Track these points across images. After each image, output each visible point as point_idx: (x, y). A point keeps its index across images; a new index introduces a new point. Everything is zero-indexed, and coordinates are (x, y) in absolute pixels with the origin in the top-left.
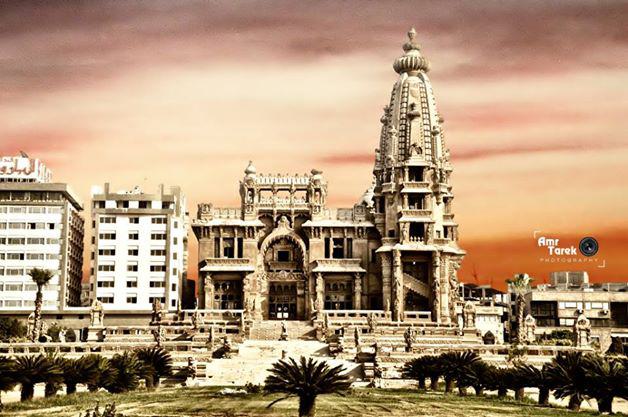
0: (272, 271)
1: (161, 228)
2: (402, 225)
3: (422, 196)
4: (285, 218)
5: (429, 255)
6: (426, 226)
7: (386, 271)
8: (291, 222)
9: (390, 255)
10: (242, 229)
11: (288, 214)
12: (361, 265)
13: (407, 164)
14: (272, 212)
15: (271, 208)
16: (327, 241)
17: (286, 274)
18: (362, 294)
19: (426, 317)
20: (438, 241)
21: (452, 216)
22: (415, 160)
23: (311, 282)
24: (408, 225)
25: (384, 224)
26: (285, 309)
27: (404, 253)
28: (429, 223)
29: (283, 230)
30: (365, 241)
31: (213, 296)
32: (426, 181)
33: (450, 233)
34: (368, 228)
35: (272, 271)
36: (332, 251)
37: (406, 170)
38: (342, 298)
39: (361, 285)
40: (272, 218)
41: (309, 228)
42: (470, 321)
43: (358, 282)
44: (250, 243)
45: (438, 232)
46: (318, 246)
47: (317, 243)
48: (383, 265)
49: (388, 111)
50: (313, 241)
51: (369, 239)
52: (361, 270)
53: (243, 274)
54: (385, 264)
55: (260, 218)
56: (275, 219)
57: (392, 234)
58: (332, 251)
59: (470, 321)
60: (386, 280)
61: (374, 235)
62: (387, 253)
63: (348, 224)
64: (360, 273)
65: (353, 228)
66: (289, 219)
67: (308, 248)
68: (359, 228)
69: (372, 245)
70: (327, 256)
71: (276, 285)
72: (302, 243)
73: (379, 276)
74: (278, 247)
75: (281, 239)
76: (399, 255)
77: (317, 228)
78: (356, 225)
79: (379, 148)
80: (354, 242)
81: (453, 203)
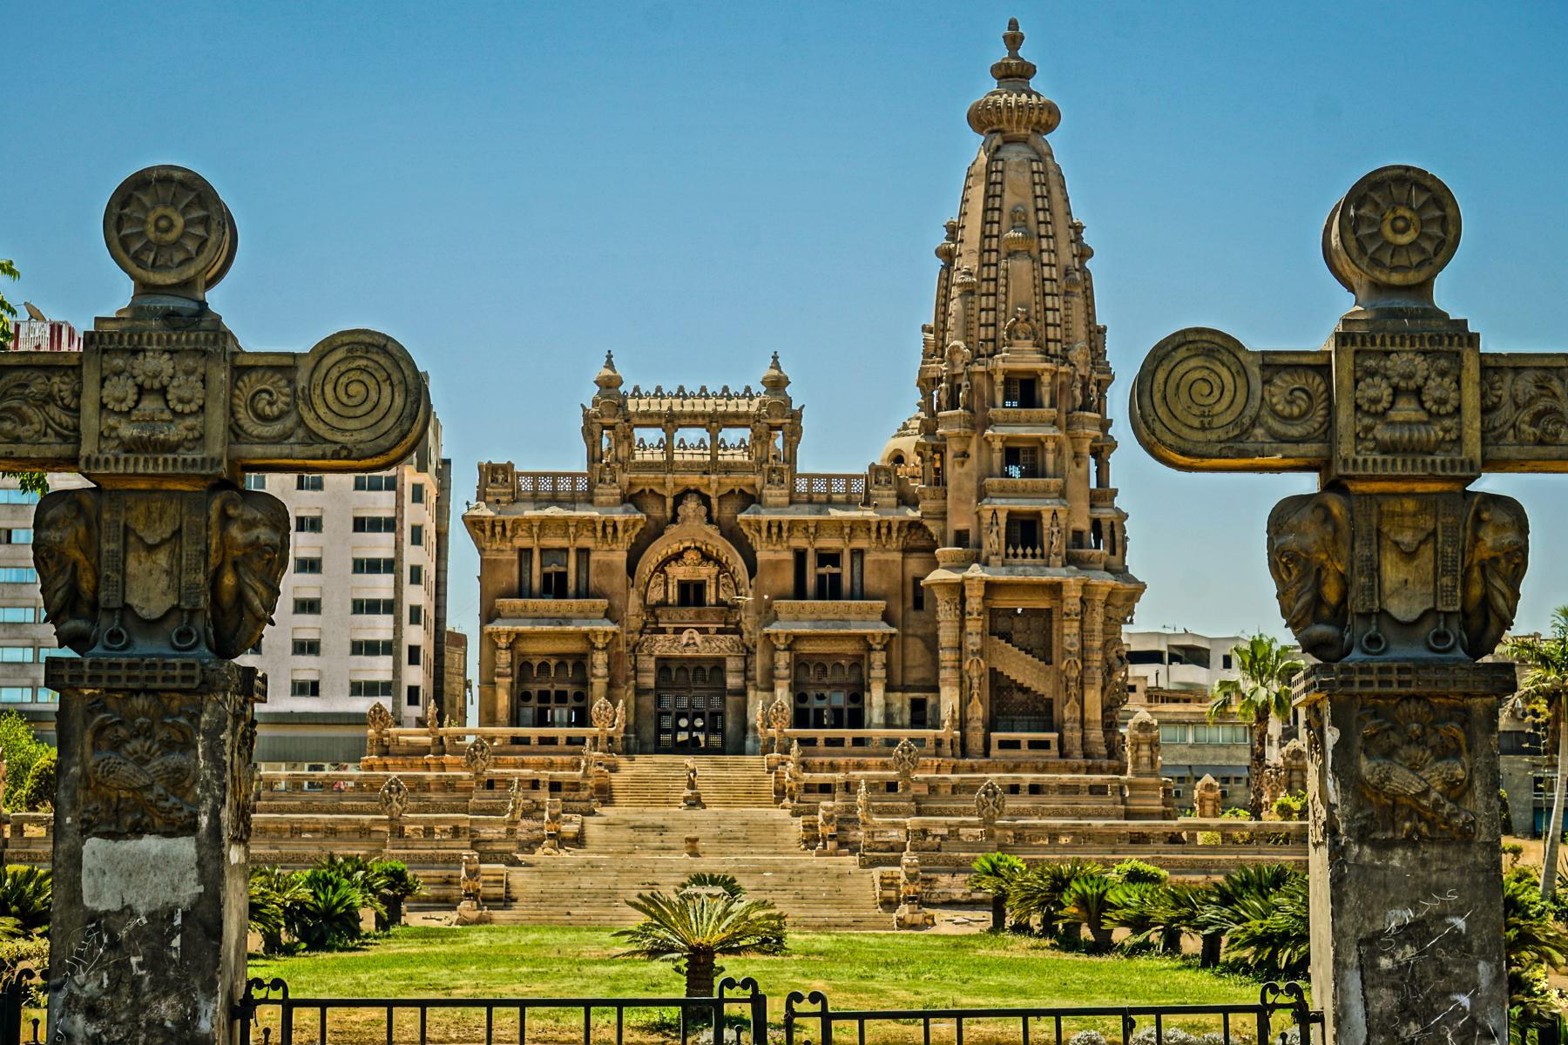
1: (381, 504)
2: (987, 516)
5: (1056, 589)
7: (947, 635)
9: (959, 589)
12: (887, 617)
16: (800, 556)
17: (698, 638)
18: (889, 688)
19: (1045, 745)
20: (1070, 560)
21: (1115, 492)
22: (1025, 358)
25: (943, 516)
26: (699, 723)
30: (898, 556)
35: (663, 631)
36: (811, 581)
38: (839, 700)
40: (663, 498)
43: (878, 658)
48: (941, 617)
49: (953, 231)
51: (906, 551)
54: (946, 615)
56: (670, 502)
57: (961, 538)
58: (811, 581)
60: (947, 657)
66: (706, 500)
67: (752, 571)
69: (914, 565)
71: (674, 667)
72: (738, 564)
73: (932, 644)
74: (678, 572)
75: (687, 549)
79: (932, 323)
80: (867, 558)
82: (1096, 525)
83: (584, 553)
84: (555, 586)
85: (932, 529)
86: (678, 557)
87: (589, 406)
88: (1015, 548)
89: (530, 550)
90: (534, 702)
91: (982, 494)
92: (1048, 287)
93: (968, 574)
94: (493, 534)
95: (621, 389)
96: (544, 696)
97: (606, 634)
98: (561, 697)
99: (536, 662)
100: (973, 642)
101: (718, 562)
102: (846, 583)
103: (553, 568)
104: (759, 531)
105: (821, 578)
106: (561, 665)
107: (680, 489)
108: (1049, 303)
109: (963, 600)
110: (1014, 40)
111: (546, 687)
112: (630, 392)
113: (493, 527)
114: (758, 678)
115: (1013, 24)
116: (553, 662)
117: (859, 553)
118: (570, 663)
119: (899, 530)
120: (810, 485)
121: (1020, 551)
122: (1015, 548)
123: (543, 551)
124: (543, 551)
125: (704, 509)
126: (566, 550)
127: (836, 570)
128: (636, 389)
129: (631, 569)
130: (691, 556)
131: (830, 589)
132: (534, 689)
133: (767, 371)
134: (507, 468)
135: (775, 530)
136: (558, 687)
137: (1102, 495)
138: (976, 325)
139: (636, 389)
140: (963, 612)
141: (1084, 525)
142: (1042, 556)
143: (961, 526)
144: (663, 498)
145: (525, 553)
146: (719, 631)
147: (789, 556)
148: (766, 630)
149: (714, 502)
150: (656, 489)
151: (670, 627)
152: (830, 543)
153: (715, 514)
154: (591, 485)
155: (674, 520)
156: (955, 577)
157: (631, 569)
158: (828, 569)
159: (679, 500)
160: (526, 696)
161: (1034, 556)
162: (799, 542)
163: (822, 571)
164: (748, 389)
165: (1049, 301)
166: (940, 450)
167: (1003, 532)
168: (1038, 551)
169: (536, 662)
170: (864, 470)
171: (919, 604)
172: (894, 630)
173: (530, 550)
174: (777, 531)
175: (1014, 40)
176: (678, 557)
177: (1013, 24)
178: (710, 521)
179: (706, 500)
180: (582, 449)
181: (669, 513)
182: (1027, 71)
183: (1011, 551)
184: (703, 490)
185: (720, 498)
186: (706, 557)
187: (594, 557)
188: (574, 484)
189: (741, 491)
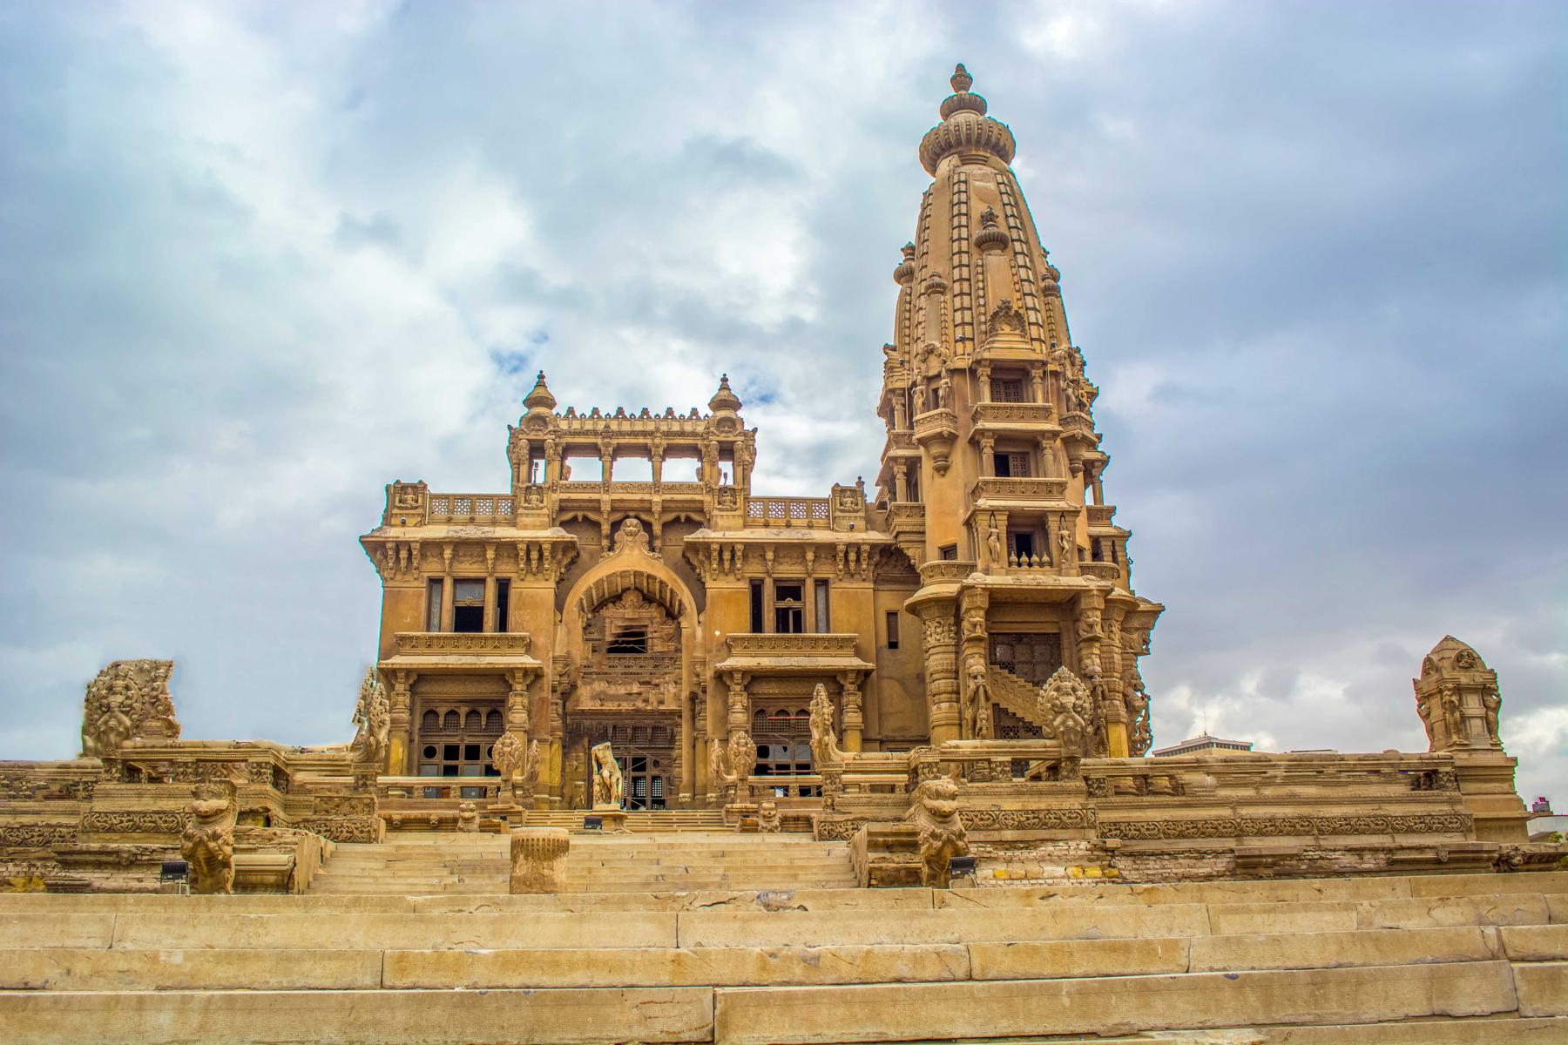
2: (982, 521)
3: (1032, 444)
4: (632, 524)
6: (1053, 523)
7: (937, 661)
8: (652, 537)
9: (951, 607)
10: (507, 548)
11: (641, 512)
13: (986, 355)
14: (596, 506)
15: (595, 496)
16: (756, 589)
20: (1084, 570)
21: (1112, 511)
22: (1009, 346)
23: (711, 707)
24: (1002, 520)
27: (998, 602)
28: (1063, 514)
29: (632, 557)
31: (419, 747)
32: (1040, 403)
33: (1107, 554)
34: (873, 546)
36: (769, 617)
37: (984, 373)
39: (862, 708)
40: (597, 525)
41: (706, 546)
42: (1476, 726)
44: (535, 590)
45: (1081, 550)
46: (729, 598)
47: (726, 587)
50: (716, 585)
52: (856, 662)
53: (502, 677)
55: (563, 524)
56: (606, 528)
57: (948, 551)
58: (769, 617)
59: (1476, 726)
61: (892, 564)
62: (938, 601)
63: (821, 536)
64: (858, 672)
65: (831, 547)
66: (647, 526)
68: (849, 545)
69: (889, 600)
70: (757, 625)
72: (686, 596)
75: (625, 590)
76: (983, 601)
77: (727, 548)
78: (843, 537)
79: (891, 343)
81: (1107, 476)
82: (1095, 541)
83: (503, 586)
84: (468, 619)
85: (909, 553)
86: (616, 598)
87: (516, 425)
88: (1019, 556)
89: (440, 581)
90: (439, 760)
91: (976, 492)
92: (1027, 288)
93: (969, 581)
94: (398, 560)
95: (554, 411)
96: (451, 752)
97: (526, 672)
98: (473, 753)
100: (976, 663)
101: (661, 604)
102: (809, 619)
103: (468, 598)
104: (709, 557)
105: (782, 615)
106: (473, 713)
107: (618, 516)
108: (1030, 305)
109: (958, 621)
110: (961, 78)
111: (454, 741)
112: (563, 414)
113: (397, 552)
114: (709, 728)
115: (960, 68)
116: (463, 710)
117: (823, 583)
118: (484, 711)
119: (870, 558)
120: (766, 510)
121: (1024, 558)
122: (1019, 556)
123: (457, 581)
124: (457, 581)
125: (646, 537)
126: (482, 581)
127: (797, 605)
128: (571, 411)
129: (559, 606)
130: (631, 598)
131: (789, 621)
132: (440, 743)
133: (711, 389)
134: (419, 488)
135: (727, 555)
136: (469, 740)
137: (1100, 514)
138: (951, 325)
139: (571, 411)
140: (958, 632)
141: (1086, 544)
142: (1051, 564)
143: (947, 541)
144: (597, 525)
145: (435, 582)
147: (744, 586)
149: (657, 529)
150: (592, 516)
152: (790, 570)
153: (658, 543)
154: (514, 509)
155: (611, 549)
156: (951, 589)
157: (559, 606)
158: (789, 602)
159: (616, 526)
160: (430, 752)
161: (1041, 564)
162: (755, 570)
163: (782, 605)
164: (694, 412)
165: (1029, 301)
166: (913, 465)
167: (1004, 536)
168: (1046, 558)
169: (442, 710)
170: (826, 493)
171: (893, 645)
172: (871, 665)
173: (440, 581)
174: (729, 554)
175: (961, 78)
176: (616, 598)
177: (960, 68)
178: (652, 549)
179: (647, 526)
180: (508, 472)
181: (605, 543)
182: (978, 105)
183: (1014, 558)
184: (644, 516)
185: (665, 525)
186: (648, 599)
188: (495, 509)
189: (688, 519)
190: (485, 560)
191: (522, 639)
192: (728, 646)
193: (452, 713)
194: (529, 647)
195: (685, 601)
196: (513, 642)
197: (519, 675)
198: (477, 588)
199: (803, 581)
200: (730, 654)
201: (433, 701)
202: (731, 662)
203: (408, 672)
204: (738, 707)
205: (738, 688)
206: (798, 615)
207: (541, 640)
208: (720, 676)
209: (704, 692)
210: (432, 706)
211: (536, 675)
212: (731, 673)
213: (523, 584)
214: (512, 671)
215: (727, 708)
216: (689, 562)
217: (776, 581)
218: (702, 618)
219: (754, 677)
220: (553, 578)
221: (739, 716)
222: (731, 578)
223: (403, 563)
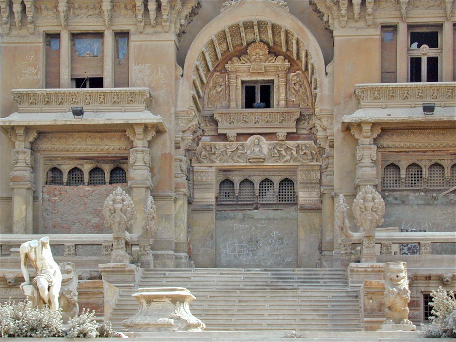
0: (224, 137)
35: (224, 137)
67: (328, 59)
71: (237, 179)
72: (312, 47)
97: (146, 127)
99: (66, 168)
101: (288, 57)
116: (87, 168)
118: (107, 168)
123: (75, 36)
124: (75, 36)
146: (290, 136)
148: (347, 119)
151: (232, 133)
157: (181, 61)
169: (66, 168)
187: (135, 41)
190: (101, 13)
191: (141, 93)
192: (356, 98)
193: (74, 171)
194: (150, 103)
195: (312, 52)
196: (132, 97)
197: (139, 130)
198: (95, 44)
199: (440, 26)
200: (358, 106)
201: (56, 158)
202: (359, 115)
203: (28, 129)
204: (367, 161)
205: (367, 141)
206: (433, 62)
207: (161, 94)
208: (347, 128)
209: (332, 146)
210: (55, 164)
211: (159, 130)
212: (359, 125)
213: (142, 37)
214: (131, 126)
215: (356, 163)
216: (317, 10)
217: (410, 27)
218: (329, 68)
219: (385, 129)
220: (174, 29)
221: (369, 171)
222: (361, 24)
223: (17, 16)
